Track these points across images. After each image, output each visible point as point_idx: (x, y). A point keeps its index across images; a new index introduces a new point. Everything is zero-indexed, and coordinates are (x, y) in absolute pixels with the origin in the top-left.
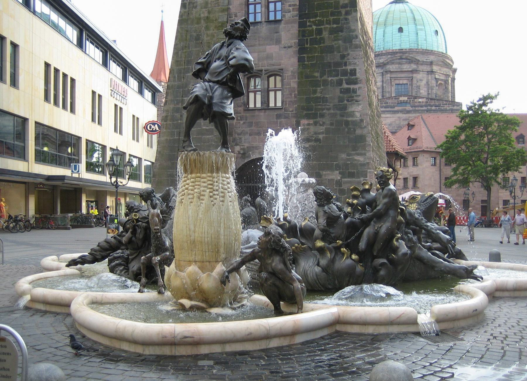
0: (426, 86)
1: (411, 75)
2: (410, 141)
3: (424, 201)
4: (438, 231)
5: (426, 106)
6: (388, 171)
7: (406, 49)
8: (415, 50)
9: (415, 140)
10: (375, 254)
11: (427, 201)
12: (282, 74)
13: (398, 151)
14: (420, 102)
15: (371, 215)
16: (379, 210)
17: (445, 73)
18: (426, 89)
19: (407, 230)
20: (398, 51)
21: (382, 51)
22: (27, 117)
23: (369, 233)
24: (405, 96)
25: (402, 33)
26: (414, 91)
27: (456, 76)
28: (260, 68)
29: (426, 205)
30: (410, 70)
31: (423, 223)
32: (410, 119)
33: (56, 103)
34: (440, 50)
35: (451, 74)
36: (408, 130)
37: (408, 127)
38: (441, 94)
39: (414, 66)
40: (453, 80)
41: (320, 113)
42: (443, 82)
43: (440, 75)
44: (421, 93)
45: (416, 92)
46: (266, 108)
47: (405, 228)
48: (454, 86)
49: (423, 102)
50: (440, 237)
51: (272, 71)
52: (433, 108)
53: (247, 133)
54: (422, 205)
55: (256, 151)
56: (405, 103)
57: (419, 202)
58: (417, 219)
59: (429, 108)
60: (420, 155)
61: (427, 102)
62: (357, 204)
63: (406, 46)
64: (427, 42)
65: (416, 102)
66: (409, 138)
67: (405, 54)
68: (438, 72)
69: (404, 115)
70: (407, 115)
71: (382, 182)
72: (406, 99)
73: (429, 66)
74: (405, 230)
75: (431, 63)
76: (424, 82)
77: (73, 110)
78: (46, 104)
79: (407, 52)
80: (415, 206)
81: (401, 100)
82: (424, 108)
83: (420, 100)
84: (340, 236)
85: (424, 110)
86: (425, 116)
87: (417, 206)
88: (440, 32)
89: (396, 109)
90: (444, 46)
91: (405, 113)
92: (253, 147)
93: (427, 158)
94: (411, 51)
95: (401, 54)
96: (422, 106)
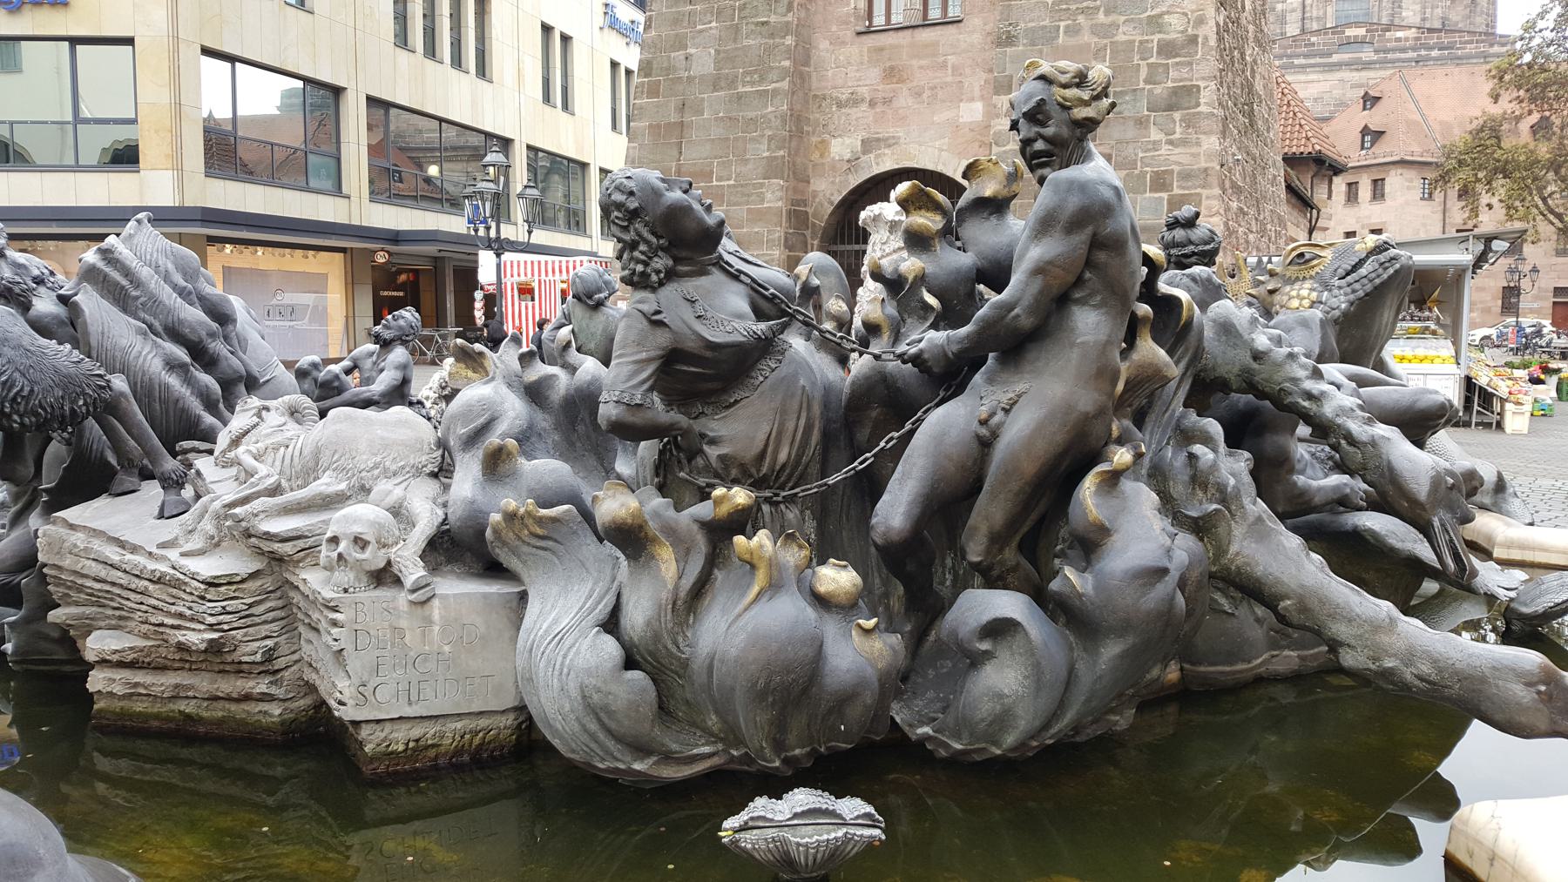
2: (1368, 138)
3: (1348, 274)
4: (1382, 430)
5: (1414, 49)
6: (1081, 80)
9: (1378, 135)
11: (1363, 271)
13: (1324, 151)
14: (1398, 40)
15: (968, 336)
16: (1008, 307)
18: (1418, 7)
19: (1192, 417)
22: (342, 84)
23: (939, 439)
24: (1357, 24)
26: (1384, 13)
29: (1357, 286)
31: (1295, 380)
32: (1371, 82)
33: (431, 51)
36: (1364, 109)
37: (1365, 102)
38: (1459, 18)
41: (1067, 27)
45: (1393, 15)
46: (921, 23)
47: (1185, 406)
49: (1407, 39)
50: (1391, 469)
52: (1435, 53)
54: (1340, 288)
55: (887, 151)
57: (1327, 275)
58: (1258, 356)
59: (1423, 53)
60: (1393, 172)
61: (1417, 39)
62: (921, 279)
65: (1389, 40)
66: (1365, 131)
69: (1355, 74)
70: (1364, 74)
71: (1039, 145)
72: (1361, 32)
74: (1183, 416)
77: (482, 71)
78: (402, 55)
80: (1304, 293)
81: (1349, 37)
82: (1411, 54)
83: (1400, 34)
84: (762, 456)
85: (1409, 60)
86: (1411, 73)
87: (1314, 295)
89: (1335, 58)
91: (1357, 70)
92: (878, 140)
93: (1411, 181)
96: (1403, 50)
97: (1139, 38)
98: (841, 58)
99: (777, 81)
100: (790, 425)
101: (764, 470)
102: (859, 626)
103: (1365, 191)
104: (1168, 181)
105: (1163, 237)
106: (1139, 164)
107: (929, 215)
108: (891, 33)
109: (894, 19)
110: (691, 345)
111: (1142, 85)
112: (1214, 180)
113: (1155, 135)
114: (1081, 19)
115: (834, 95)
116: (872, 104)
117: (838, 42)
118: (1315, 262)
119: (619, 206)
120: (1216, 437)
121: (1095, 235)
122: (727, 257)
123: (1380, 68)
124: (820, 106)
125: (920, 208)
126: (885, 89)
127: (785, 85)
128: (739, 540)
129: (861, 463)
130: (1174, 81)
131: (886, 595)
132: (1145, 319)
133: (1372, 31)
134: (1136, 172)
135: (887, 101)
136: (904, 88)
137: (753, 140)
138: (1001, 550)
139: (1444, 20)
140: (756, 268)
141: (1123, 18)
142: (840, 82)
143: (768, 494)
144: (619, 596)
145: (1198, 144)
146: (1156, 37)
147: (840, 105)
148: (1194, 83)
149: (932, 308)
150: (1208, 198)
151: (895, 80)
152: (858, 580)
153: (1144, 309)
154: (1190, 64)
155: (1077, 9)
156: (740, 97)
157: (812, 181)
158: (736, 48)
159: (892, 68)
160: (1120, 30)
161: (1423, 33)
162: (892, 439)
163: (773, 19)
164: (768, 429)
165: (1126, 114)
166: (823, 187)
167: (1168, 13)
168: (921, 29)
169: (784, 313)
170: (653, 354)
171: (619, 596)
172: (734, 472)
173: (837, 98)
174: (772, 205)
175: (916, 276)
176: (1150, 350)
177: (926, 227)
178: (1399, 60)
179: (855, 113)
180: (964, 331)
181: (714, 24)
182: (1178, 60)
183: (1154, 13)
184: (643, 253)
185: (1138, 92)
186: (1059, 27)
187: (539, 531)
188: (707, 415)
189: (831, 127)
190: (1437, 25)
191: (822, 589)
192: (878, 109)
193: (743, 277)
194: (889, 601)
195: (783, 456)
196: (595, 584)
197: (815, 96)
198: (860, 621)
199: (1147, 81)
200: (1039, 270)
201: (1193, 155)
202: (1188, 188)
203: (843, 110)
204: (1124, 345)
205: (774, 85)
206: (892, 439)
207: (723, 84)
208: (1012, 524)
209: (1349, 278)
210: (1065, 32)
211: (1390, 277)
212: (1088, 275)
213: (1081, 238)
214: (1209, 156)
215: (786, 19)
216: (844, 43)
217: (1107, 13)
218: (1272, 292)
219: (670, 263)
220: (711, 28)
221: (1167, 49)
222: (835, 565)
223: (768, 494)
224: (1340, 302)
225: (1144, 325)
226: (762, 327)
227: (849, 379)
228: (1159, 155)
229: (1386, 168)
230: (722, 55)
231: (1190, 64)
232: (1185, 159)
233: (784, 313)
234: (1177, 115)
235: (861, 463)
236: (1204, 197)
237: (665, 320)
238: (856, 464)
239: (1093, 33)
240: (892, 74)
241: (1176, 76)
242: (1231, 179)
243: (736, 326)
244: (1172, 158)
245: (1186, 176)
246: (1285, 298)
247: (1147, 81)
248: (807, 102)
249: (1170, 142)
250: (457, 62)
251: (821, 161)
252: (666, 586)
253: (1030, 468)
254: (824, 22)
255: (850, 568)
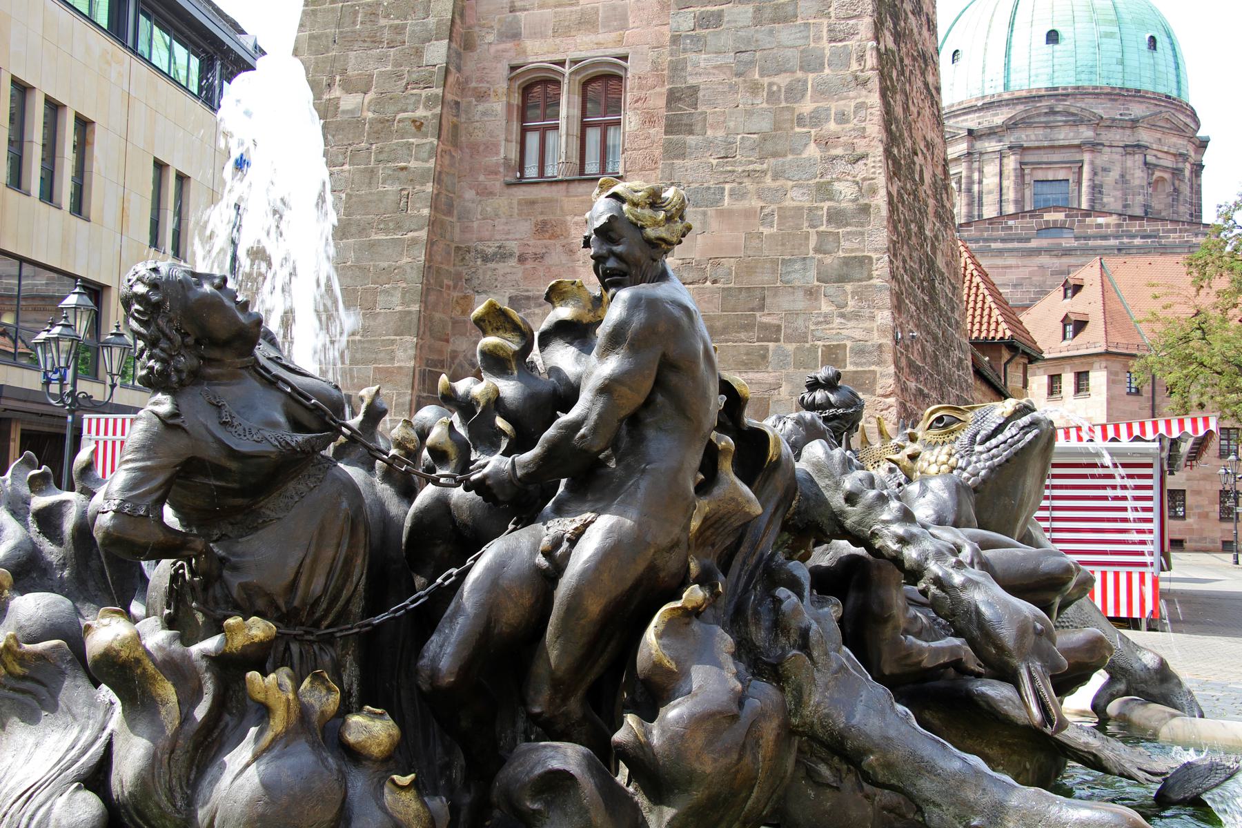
0: (1119, 186)
1: (1078, 157)
3: (989, 438)
5: (1116, 237)
7: (1065, 88)
8: (1091, 91)
10: (537, 710)
12: (622, 73)
13: (1016, 336)
14: (1099, 226)
15: (533, 460)
16: (576, 425)
17: (1172, 151)
18: (1119, 194)
20: (1043, 93)
21: (1000, 95)
24: (1056, 209)
25: (1056, 47)
27: (1207, 159)
28: (558, 57)
30: (1077, 142)
34: (1161, 90)
35: (1192, 154)
37: (1065, 290)
39: (1087, 133)
40: (1198, 168)
41: (732, 190)
42: (1167, 176)
43: (1160, 155)
44: (1104, 205)
46: (578, 177)
48: (1200, 186)
49: (1108, 226)
51: (594, 64)
53: (511, 255)
55: (537, 311)
56: (1058, 227)
59: (1125, 240)
60: (1096, 365)
61: (1119, 226)
63: (1066, 80)
64: (1127, 70)
65: (1090, 226)
66: (1065, 321)
67: (1065, 100)
68: (1155, 146)
71: (611, 263)
73: (1128, 132)
75: (1134, 123)
76: (1115, 174)
79: (1067, 95)
81: (1047, 222)
82: (1112, 242)
83: (1100, 220)
84: (293, 586)
88: (1162, 42)
89: (1034, 244)
90: (1172, 78)
91: (1057, 256)
92: (528, 298)
94: (1079, 92)
95: (1053, 102)
96: (1105, 237)
97: (807, 204)
98: (488, 209)
99: (415, 230)
100: (329, 553)
101: (296, 603)
102: (393, 781)
103: (1068, 381)
104: (840, 357)
105: (803, 398)
106: (810, 338)
107: (507, 336)
108: (544, 186)
109: (550, 172)
110: (211, 453)
111: (811, 253)
112: (889, 357)
113: (825, 307)
114: (747, 183)
115: (479, 248)
116: (522, 259)
117: (485, 193)
118: (955, 426)
119: (141, 298)
120: (803, 579)
121: (664, 355)
122: (263, 361)
123: (1081, 255)
124: (463, 259)
125: (498, 329)
126: (536, 245)
127: (423, 234)
128: (254, 675)
129: (413, 602)
130: (845, 251)
131: (448, 766)
132: (725, 450)
133: (1071, 216)
134: (807, 345)
135: (539, 257)
136: (558, 243)
137: (386, 292)
138: (565, 700)
139: (1146, 207)
140: (299, 377)
141: (790, 183)
142: (486, 234)
143: (298, 631)
144: (109, 746)
145: (873, 318)
146: (826, 205)
147: (486, 259)
148: (866, 254)
149: (504, 433)
150: (882, 375)
151: (547, 235)
152: (395, 731)
153: (726, 442)
154: (862, 234)
155: (744, 171)
156: (373, 245)
157: (451, 340)
158: (371, 193)
159: (544, 223)
160: (788, 195)
161: (1125, 220)
162: (450, 576)
163: (413, 164)
164: (301, 555)
165: (797, 283)
166: (464, 347)
167: (838, 179)
168: (576, 183)
169: (330, 428)
170: (165, 461)
171: (109, 746)
172: (260, 603)
173: (483, 251)
174: (402, 364)
175: (489, 400)
176: (732, 484)
177: (502, 348)
178: (1100, 247)
179: (502, 267)
180: (528, 456)
181: (346, 167)
182: (849, 229)
183: (822, 180)
184: (163, 350)
185: (808, 261)
186: (723, 189)
187: (18, 670)
188: (229, 537)
189: (475, 282)
190: (1138, 211)
191: (351, 738)
192: (529, 265)
193: (281, 384)
194: (451, 773)
195: (318, 585)
196: (82, 731)
197: (458, 248)
198: (395, 777)
199: (817, 250)
200: (606, 389)
201: (865, 329)
202: (862, 365)
203: (490, 265)
204: (701, 477)
205: (410, 234)
206: (450, 576)
207: (353, 229)
208: (579, 667)
209: (988, 444)
210: (731, 195)
211: (1030, 442)
212: (660, 398)
213: (652, 359)
214: (882, 331)
215: (427, 165)
216: (492, 194)
217: (775, 178)
218: (913, 457)
219: (195, 362)
220: (342, 171)
221: (836, 217)
222: (370, 712)
223: (298, 631)
224: (980, 464)
225: (725, 457)
226: (300, 437)
227: (412, 511)
228: (830, 329)
229: (1090, 360)
230: (354, 199)
231: (862, 234)
232: (858, 334)
233: (330, 428)
234: (849, 287)
235: (413, 602)
236: (878, 375)
237: (183, 425)
238: (407, 602)
239: (759, 197)
240: (543, 228)
241: (848, 247)
242: (907, 357)
243: (267, 434)
244: (845, 332)
245: (860, 352)
246: (925, 464)
247: (817, 250)
248: (449, 254)
249: (842, 316)
250: (48, 195)
251: (462, 318)
252: (163, 732)
253: (594, 607)
254: (471, 169)
255: (388, 716)
